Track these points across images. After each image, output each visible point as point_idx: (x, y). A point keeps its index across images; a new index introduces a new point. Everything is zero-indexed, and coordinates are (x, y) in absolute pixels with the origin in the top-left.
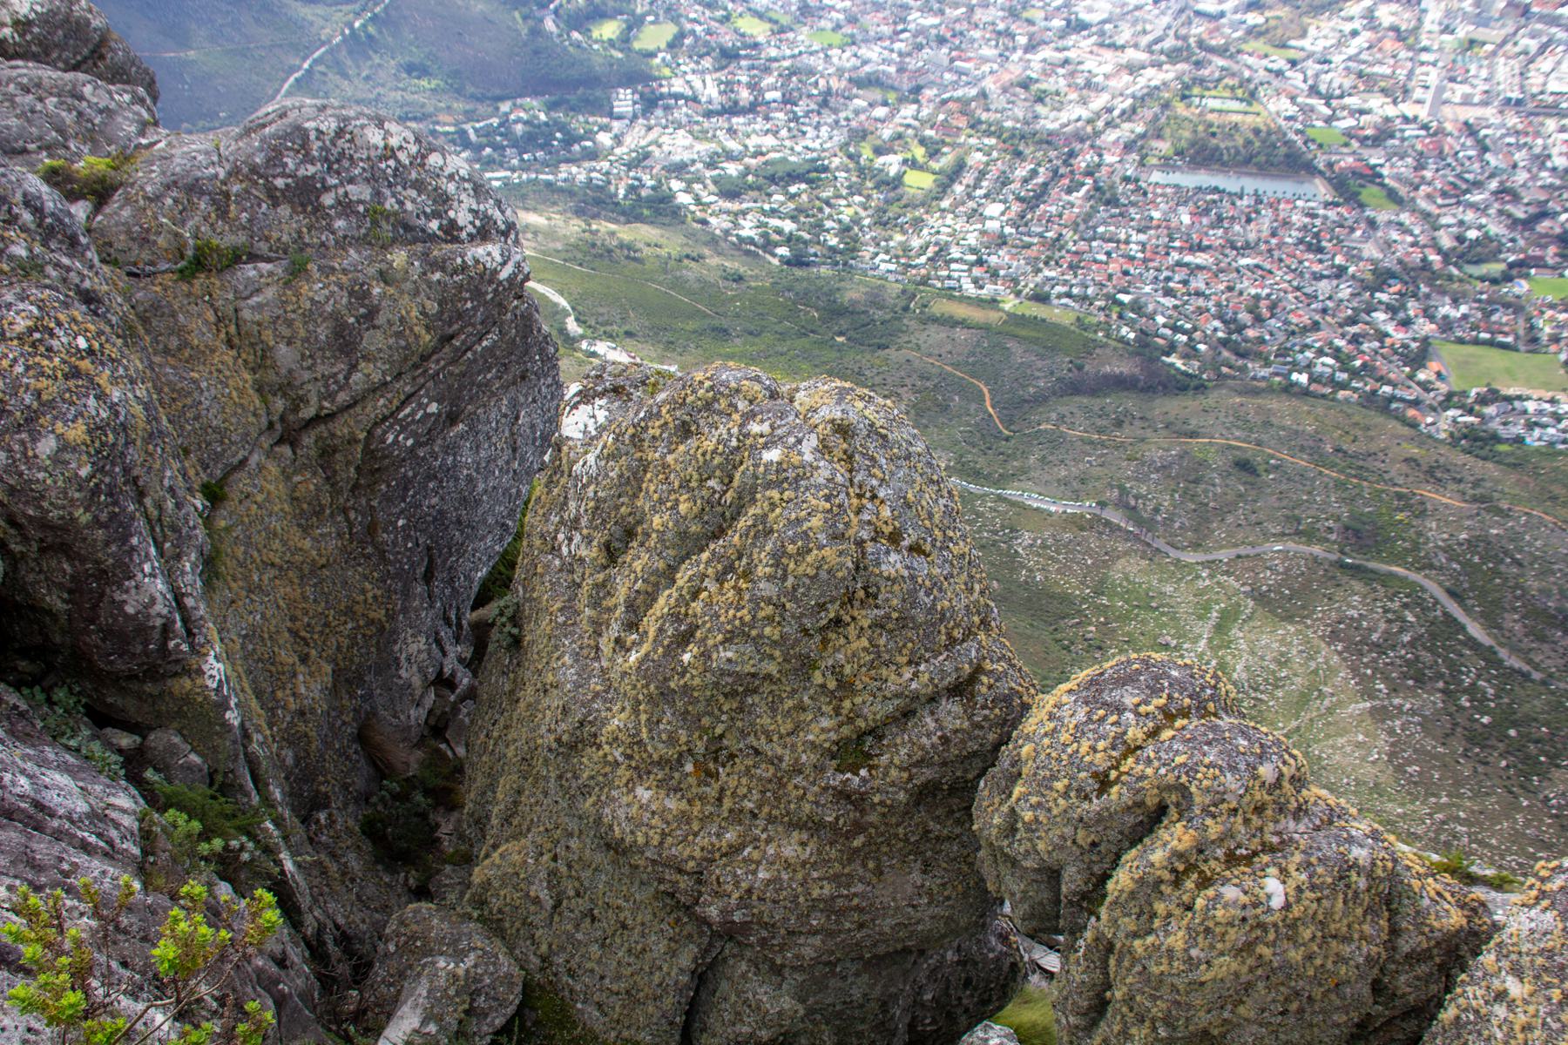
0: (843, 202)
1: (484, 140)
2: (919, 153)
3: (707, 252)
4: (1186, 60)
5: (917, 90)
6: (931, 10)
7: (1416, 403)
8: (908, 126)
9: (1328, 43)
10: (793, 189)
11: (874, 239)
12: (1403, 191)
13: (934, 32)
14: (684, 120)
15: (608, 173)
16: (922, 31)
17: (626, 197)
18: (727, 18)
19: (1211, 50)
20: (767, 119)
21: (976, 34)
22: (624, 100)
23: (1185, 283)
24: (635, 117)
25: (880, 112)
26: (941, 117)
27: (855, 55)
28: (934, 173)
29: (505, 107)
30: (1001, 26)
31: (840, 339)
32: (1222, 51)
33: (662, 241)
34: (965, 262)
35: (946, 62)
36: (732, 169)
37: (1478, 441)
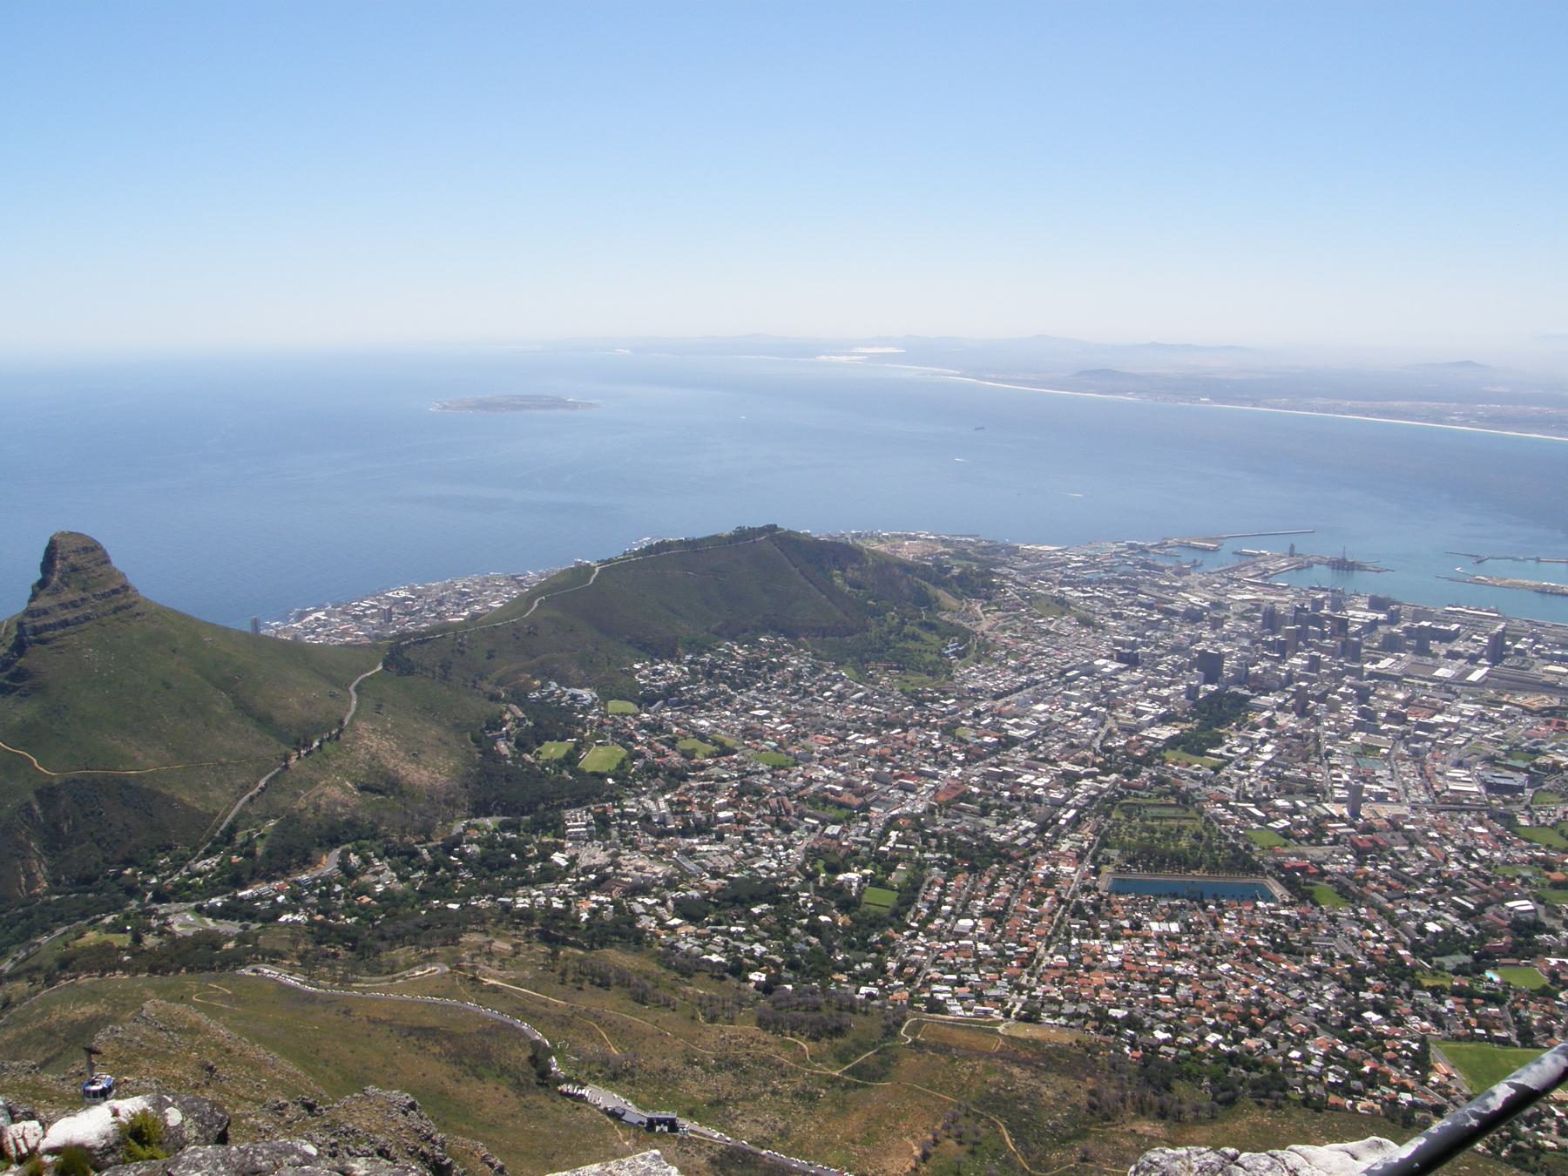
4: (1118, 772)
5: (865, 807)
6: (869, 730)
9: (1245, 749)
10: (756, 910)
12: (1354, 888)
19: (1138, 760)
22: (577, 820)
23: (1171, 992)
28: (892, 889)
32: (1146, 761)
34: (947, 982)
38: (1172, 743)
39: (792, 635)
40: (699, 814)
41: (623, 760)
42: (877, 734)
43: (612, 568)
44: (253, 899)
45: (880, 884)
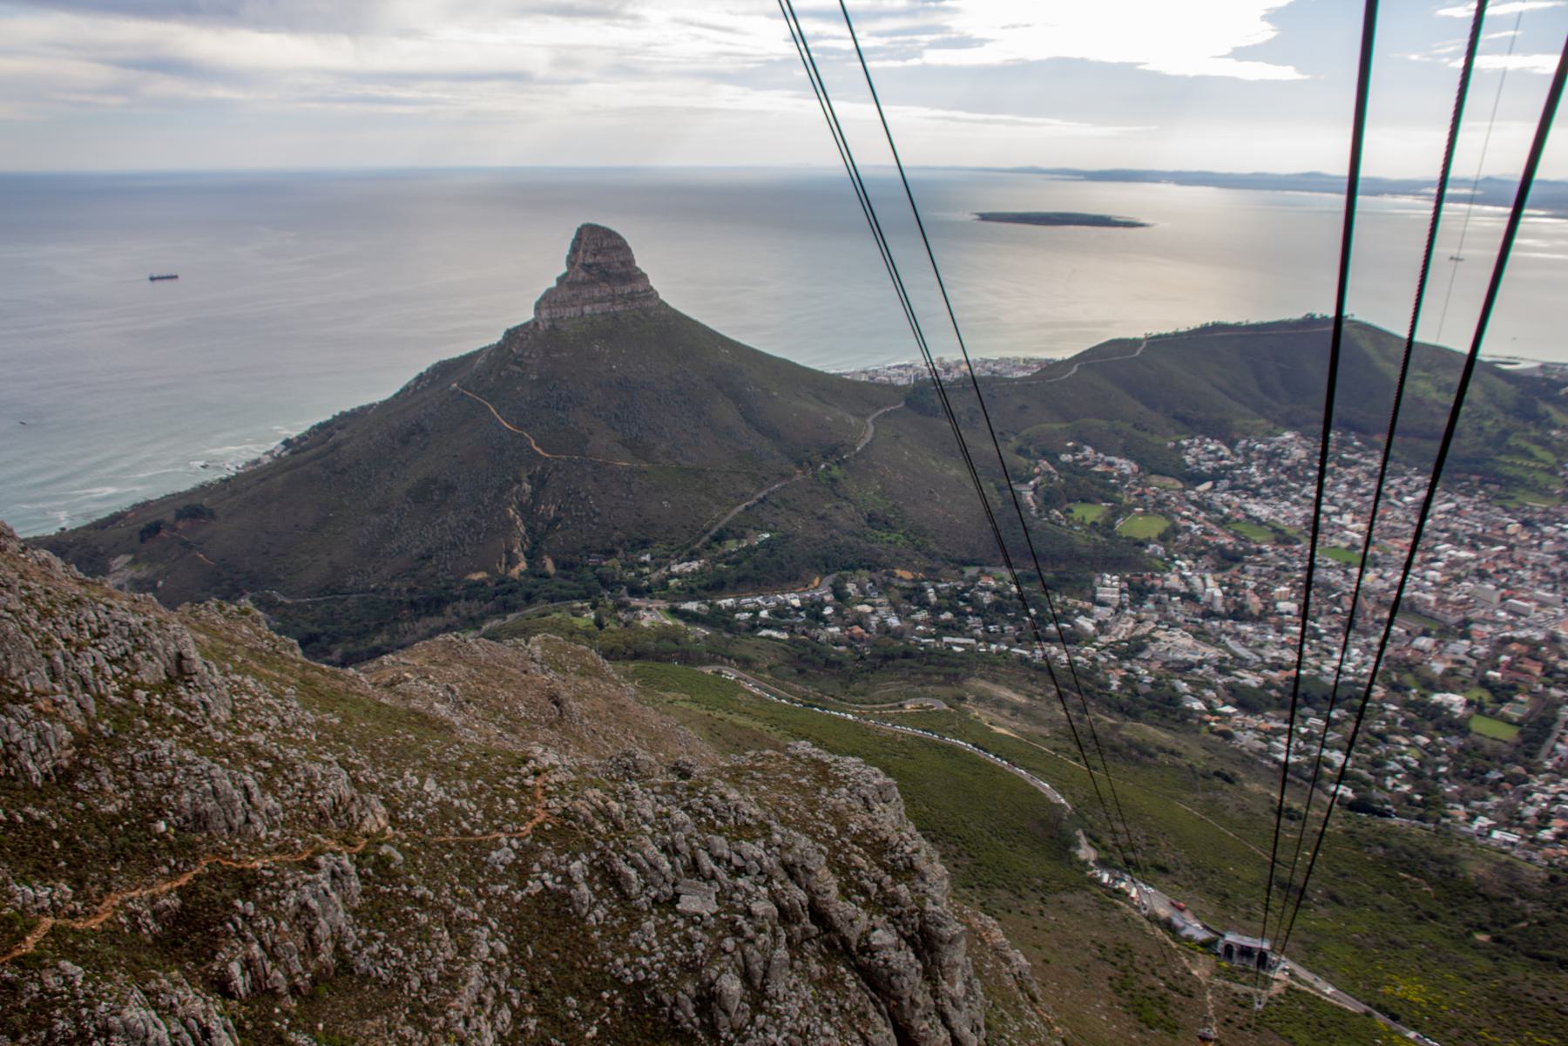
0: (1404, 741)
1: (945, 602)
2: (1486, 696)
3: (1242, 776)
5: (1466, 622)
8: (1462, 663)
11: (1462, 793)
13: (1473, 565)
14: (1180, 619)
15: (1094, 660)
16: (1454, 563)
17: (1120, 688)
20: (1280, 630)
21: (1525, 574)
22: (1110, 587)
24: (1120, 609)
25: (1423, 642)
26: (1504, 658)
27: (1381, 577)
28: (1509, 722)
29: (971, 571)
30: (1556, 570)
31: (1482, 937)
33: (1179, 749)
35: (1496, 598)
40: (1256, 599)
41: (1167, 530)
42: (1473, 547)
43: (1158, 343)
44: (733, 610)
45: (1493, 715)
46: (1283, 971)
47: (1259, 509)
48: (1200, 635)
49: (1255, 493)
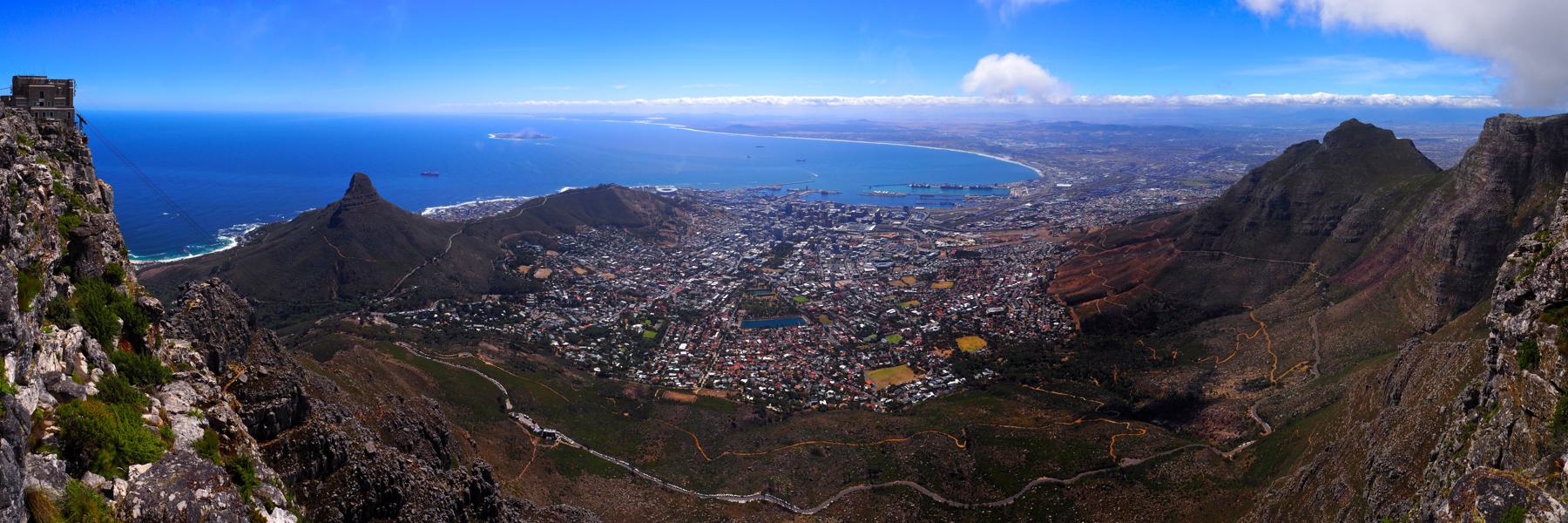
7: (869, 401)
16: (645, 273)
18: (570, 268)
36: (574, 330)
37: (894, 407)
38: (765, 265)
39: (619, 226)
46: (560, 437)
47: (583, 261)
48: (560, 314)
49: (583, 254)
